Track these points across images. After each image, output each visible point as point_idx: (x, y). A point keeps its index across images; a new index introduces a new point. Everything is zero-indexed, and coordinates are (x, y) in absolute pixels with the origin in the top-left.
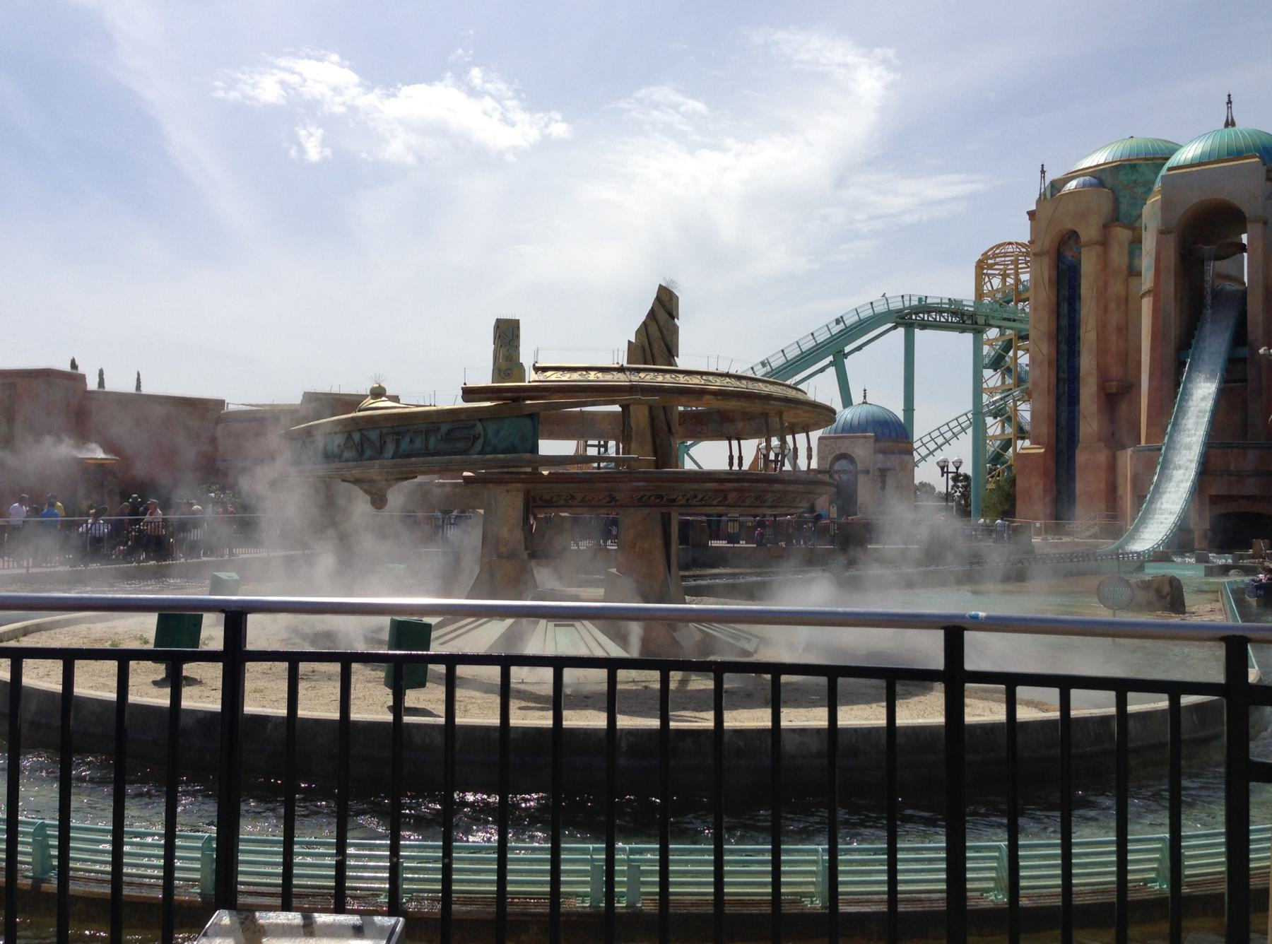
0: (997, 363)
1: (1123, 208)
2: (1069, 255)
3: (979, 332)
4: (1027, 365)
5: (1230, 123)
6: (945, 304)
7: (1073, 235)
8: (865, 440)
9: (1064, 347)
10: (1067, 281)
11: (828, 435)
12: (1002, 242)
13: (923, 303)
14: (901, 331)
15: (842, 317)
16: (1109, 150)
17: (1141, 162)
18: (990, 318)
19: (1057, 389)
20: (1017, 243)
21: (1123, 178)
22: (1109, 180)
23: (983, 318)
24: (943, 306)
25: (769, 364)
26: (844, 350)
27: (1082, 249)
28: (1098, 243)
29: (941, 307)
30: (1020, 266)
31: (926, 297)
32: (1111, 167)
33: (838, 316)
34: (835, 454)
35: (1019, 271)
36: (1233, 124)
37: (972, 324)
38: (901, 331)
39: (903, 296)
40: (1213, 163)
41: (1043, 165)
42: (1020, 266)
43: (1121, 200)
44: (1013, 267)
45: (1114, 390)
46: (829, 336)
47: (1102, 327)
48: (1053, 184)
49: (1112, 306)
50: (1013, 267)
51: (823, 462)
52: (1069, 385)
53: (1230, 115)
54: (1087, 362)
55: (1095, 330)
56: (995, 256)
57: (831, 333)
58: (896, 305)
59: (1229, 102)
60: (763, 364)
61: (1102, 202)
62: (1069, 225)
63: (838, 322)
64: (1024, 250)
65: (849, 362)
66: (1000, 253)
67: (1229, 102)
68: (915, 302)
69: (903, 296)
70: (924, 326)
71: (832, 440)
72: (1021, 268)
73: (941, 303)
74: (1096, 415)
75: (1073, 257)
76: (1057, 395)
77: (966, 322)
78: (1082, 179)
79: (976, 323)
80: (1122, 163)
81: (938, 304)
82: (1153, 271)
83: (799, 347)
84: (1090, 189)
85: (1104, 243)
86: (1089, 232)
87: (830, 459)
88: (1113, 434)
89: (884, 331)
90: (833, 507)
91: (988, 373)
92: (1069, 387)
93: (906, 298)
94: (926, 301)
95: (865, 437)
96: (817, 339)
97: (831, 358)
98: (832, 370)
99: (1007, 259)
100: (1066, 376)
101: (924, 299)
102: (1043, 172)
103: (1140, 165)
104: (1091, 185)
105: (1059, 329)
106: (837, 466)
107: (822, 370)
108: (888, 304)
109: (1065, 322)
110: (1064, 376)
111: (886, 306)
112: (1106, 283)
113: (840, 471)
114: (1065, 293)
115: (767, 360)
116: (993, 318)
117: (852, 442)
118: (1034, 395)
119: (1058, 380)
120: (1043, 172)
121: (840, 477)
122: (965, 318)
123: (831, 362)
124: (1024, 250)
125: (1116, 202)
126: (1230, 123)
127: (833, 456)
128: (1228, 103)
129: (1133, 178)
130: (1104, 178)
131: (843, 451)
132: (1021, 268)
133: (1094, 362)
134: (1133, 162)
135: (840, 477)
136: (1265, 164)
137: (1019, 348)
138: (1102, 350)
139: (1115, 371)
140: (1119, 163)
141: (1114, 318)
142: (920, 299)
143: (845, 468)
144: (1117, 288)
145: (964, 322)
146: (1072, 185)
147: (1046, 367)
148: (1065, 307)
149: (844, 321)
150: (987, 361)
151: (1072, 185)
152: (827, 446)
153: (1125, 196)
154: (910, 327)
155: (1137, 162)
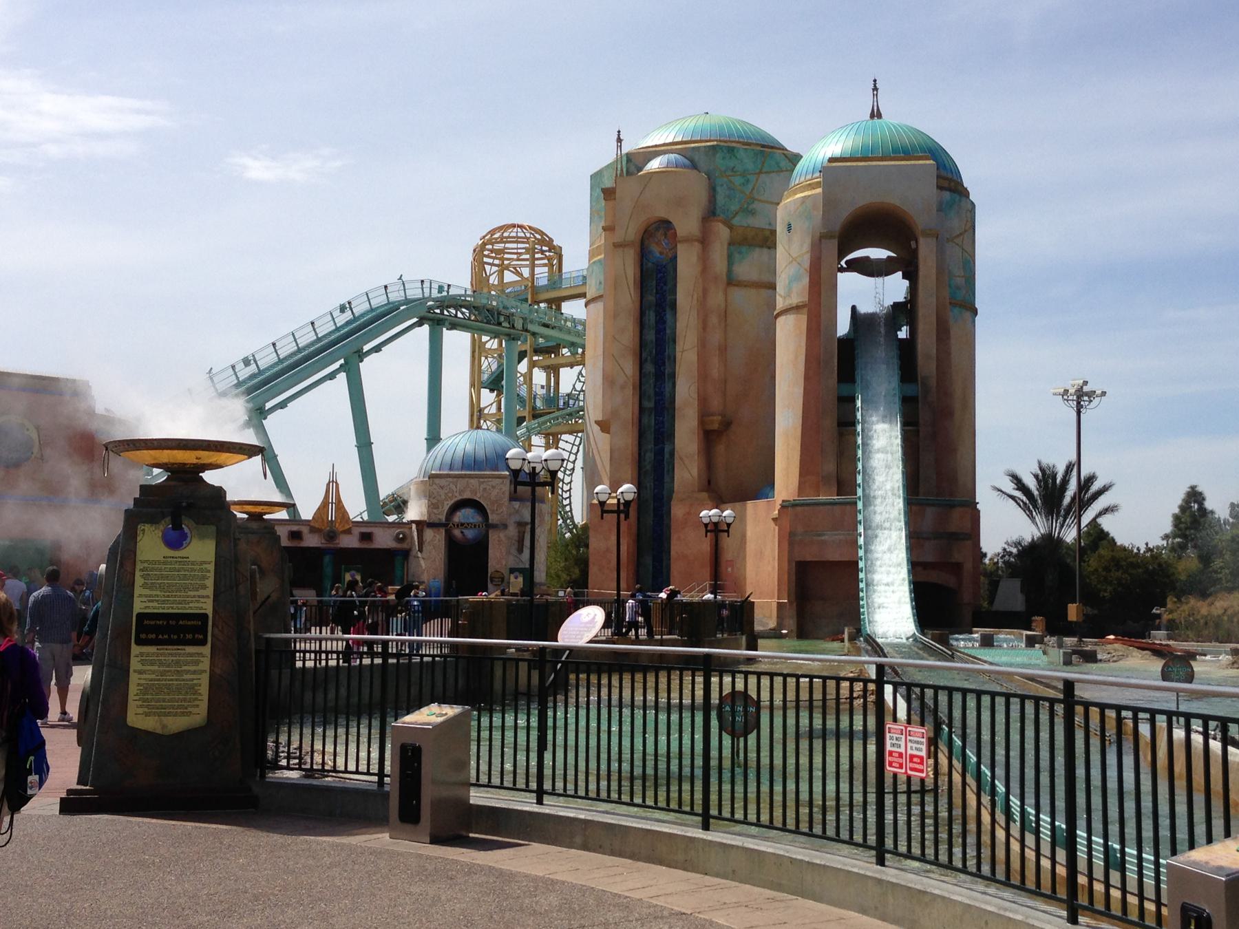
0: (495, 384)
1: (721, 199)
2: (656, 250)
3: (513, 339)
4: (542, 387)
5: (876, 114)
6: (469, 296)
7: (665, 225)
8: (501, 480)
9: (649, 368)
10: (655, 282)
11: (438, 472)
12: (510, 223)
13: (445, 294)
14: (426, 328)
15: (349, 303)
16: (677, 128)
17: (738, 145)
18: (528, 321)
19: (640, 421)
20: (530, 227)
21: (720, 161)
22: (702, 161)
23: (521, 321)
24: (467, 299)
25: (255, 362)
26: (362, 349)
27: (679, 246)
28: (697, 240)
29: (465, 300)
30: (537, 256)
31: (449, 286)
32: (705, 147)
33: (344, 301)
34: (456, 499)
35: (536, 262)
36: (879, 116)
37: (509, 328)
38: (426, 328)
39: (422, 281)
40: (881, 159)
41: (619, 132)
42: (537, 256)
43: (719, 189)
44: (528, 256)
45: (716, 426)
46: (334, 327)
47: (703, 344)
48: (630, 157)
49: (714, 320)
50: (528, 256)
51: (435, 511)
52: (655, 416)
53: (875, 104)
54: (685, 390)
55: (696, 349)
56: (502, 240)
57: (335, 324)
58: (414, 293)
59: (875, 89)
60: (246, 362)
61: (696, 186)
62: (662, 213)
63: (342, 309)
64: (538, 236)
65: (367, 367)
66: (509, 237)
67: (875, 89)
68: (435, 294)
69: (422, 281)
70: (453, 326)
71: (450, 479)
72: (538, 259)
73: (465, 295)
74: (696, 457)
75: (661, 253)
76: (640, 429)
77: (503, 324)
78: (672, 156)
79: (513, 327)
80: (719, 143)
81: (460, 296)
82: (806, 280)
83: (295, 340)
84: (685, 170)
85: (704, 241)
86: (687, 224)
87: (446, 508)
88: (709, 482)
89: (403, 330)
90: (516, 578)
91: (485, 393)
92: (655, 420)
93: (426, 285)
94: (448, 292)
95: (499, 477)
96: (318, 331)
97: (342, 361)
98: (342, 376)
99: (520, 245)
100: (651, 405)
101: (446, 289)
102: (619, 140)
103: (738, 149)
104: (685, 166)
105: (642, 344)
106: (459, 516)
107: (331, 376)
108: (405, 290)
109: (651, 336)
110: (649, 404)
111: (402, 293)
112: (705, 292)
113: (462, 524)
114: (651, 298)
115: (253, 356)
116: (531, 322)
117: (481, 483)
118: (613, 429)
119: (642, 409)
120: (619, 140)
121: (462, 532)
122: (502, 319)
123: (341, 366)
124: (538, 236)
125: (712, 190)
126: (876, 114)
127: (453, 502)
128: (873, 90)
129: (731, 164)
130: (696, 158)
131: (467, 495)
132: (538, 259)
133: (694, 388)
134: (729, 144)
135: (462, 532)
136: (938, 169)
137: (532, 365)
138: (703, 376)
139: (715, 403)
140: (715, 143)
141: (715, 337)
142: (441, 289)
143: (471, 521)
144: (716, 298)
145: (499, 324)
146: (655, 165)
147: (629, 391)
148: (651, 317)
149: (351, 309)
150: (485, 377)
151: (655, 165)
152: (442, 488)
153: (722, 185)
154: (438, 324)
155: (734, 145)
